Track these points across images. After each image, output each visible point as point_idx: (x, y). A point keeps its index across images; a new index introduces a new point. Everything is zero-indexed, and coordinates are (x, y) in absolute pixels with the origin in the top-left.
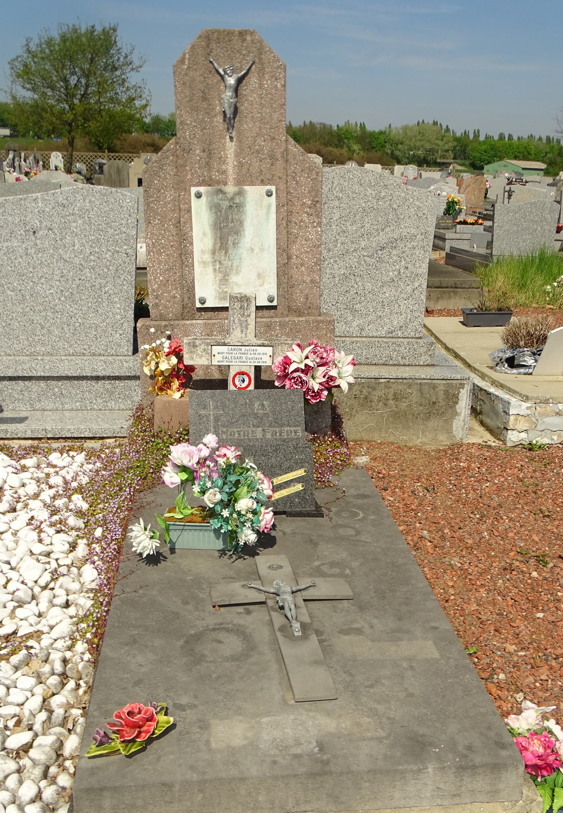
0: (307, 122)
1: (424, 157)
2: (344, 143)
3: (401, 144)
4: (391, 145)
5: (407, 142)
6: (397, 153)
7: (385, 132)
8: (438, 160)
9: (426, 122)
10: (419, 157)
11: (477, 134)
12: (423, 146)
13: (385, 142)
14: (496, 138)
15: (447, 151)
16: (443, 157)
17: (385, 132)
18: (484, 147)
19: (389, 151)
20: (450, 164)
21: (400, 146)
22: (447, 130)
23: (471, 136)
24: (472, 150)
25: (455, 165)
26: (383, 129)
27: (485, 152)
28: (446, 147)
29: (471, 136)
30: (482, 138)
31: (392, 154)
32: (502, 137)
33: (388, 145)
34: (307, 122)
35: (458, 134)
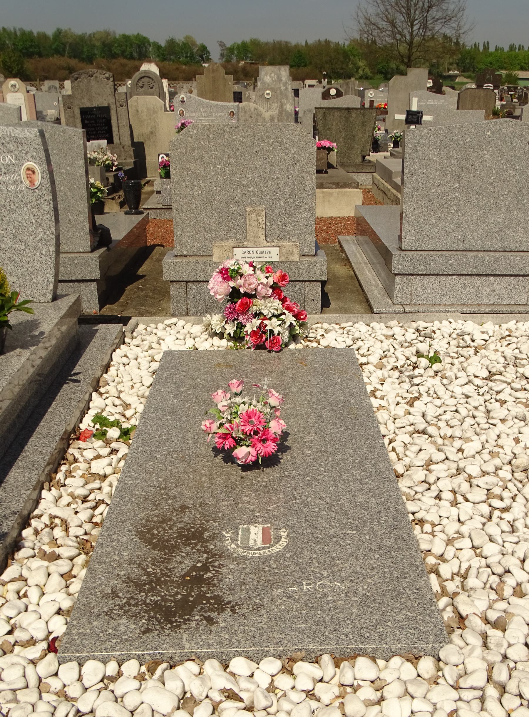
2: (350, 60)
8: (444, 74)
18: (490, 59)
20: (456, 76)
24: (478, 62)
25: (461, 78)
27: (491, 63)
31: (397, 69)
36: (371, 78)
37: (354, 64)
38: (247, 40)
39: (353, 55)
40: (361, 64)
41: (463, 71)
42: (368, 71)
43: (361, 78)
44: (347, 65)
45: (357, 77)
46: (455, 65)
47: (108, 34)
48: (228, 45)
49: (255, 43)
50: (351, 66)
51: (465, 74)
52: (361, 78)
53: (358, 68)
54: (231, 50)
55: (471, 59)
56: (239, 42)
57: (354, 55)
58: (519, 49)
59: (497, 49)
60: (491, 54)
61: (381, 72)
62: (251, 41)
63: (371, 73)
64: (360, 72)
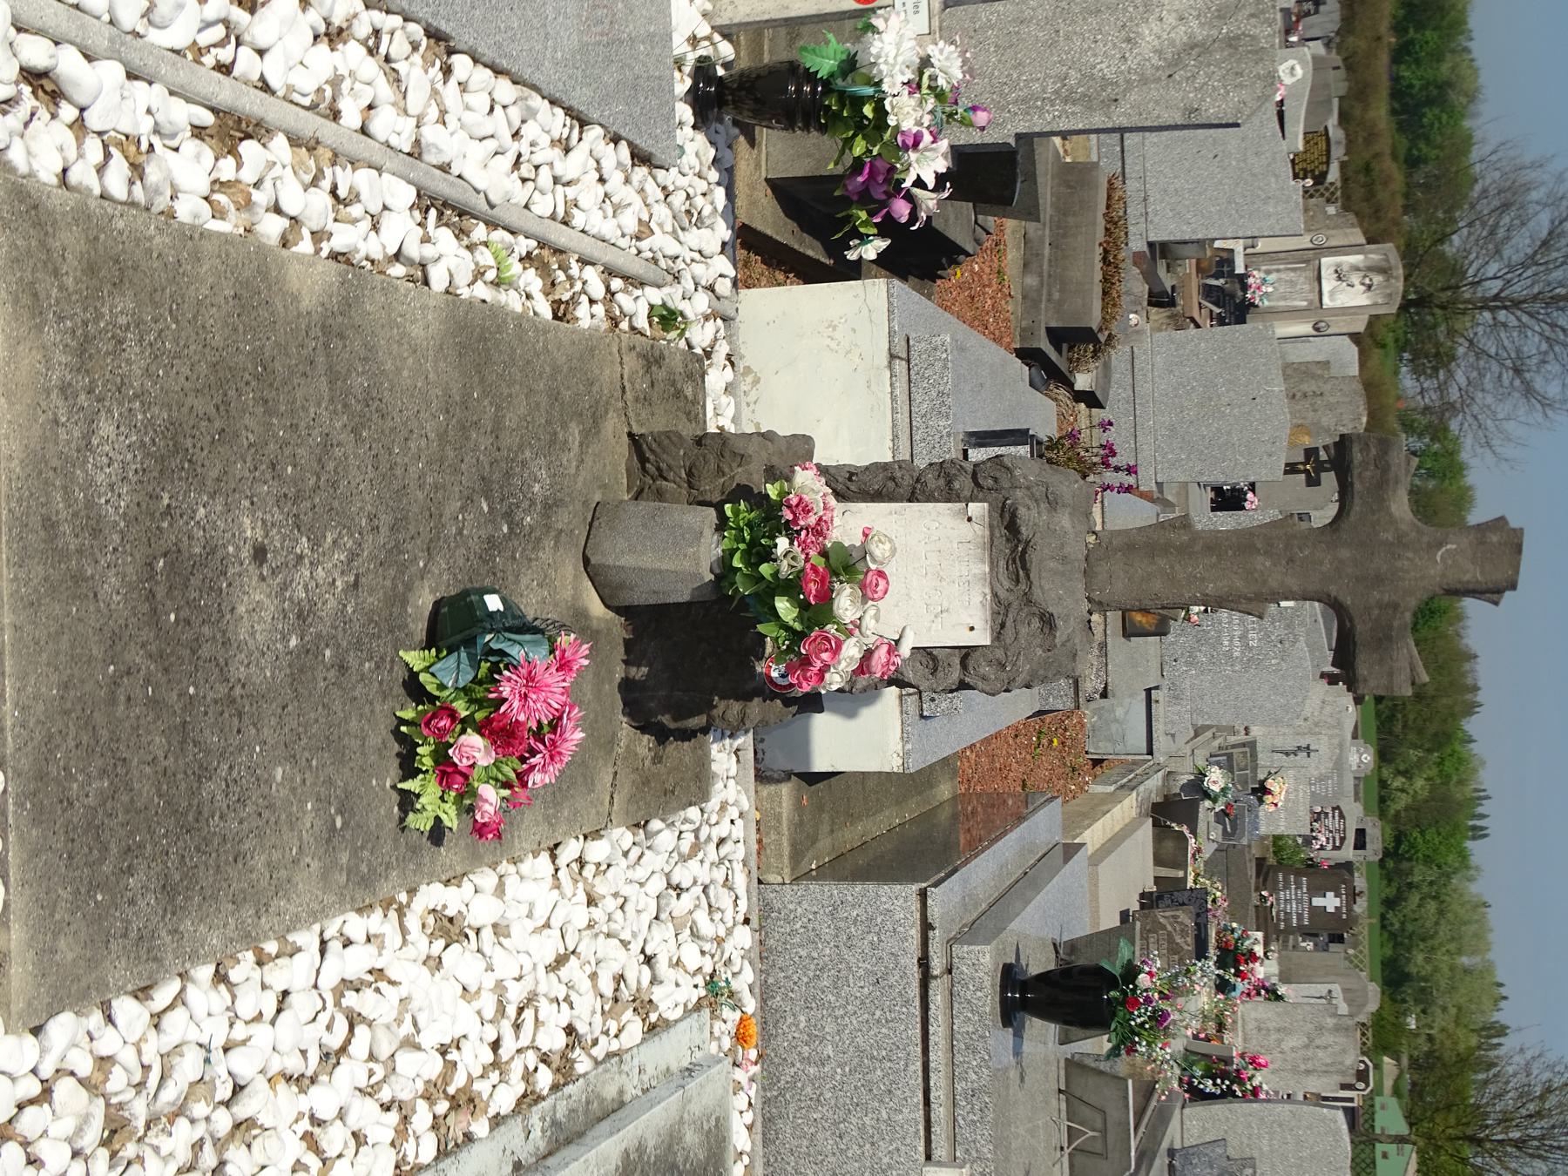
1: (1406, 977)
2: (1429, 751)
3: (1441, 913)
4: (1431, 883)
5: (1444, 930)
6: (1415, 898)
7: (1468, 867)
9: (1503, 1004)
10: (1408, 960)
12: (1436, 970)
13: (1439, 867)
17: (1468, 867)
19: (1417, 878)
21: (1432, 906)
25: (1395, 1071)
26: (1474, 860)
31: (1410, 885)
33: (1432, 874)
37: (1420, 764)
39: (1440, 763)
40: (1419, 783)
42: (1401, 802)
43: (1383, 784)
44: (1416, 747)
45: (1385, 773)
50: (1414, 754)
52: (1383, 784)
53: (1407, 774)
57: (1440, 763)
61: (1398, 840)
62: (1470, 488)
63: (1398, 813)
64: (1398, 782)
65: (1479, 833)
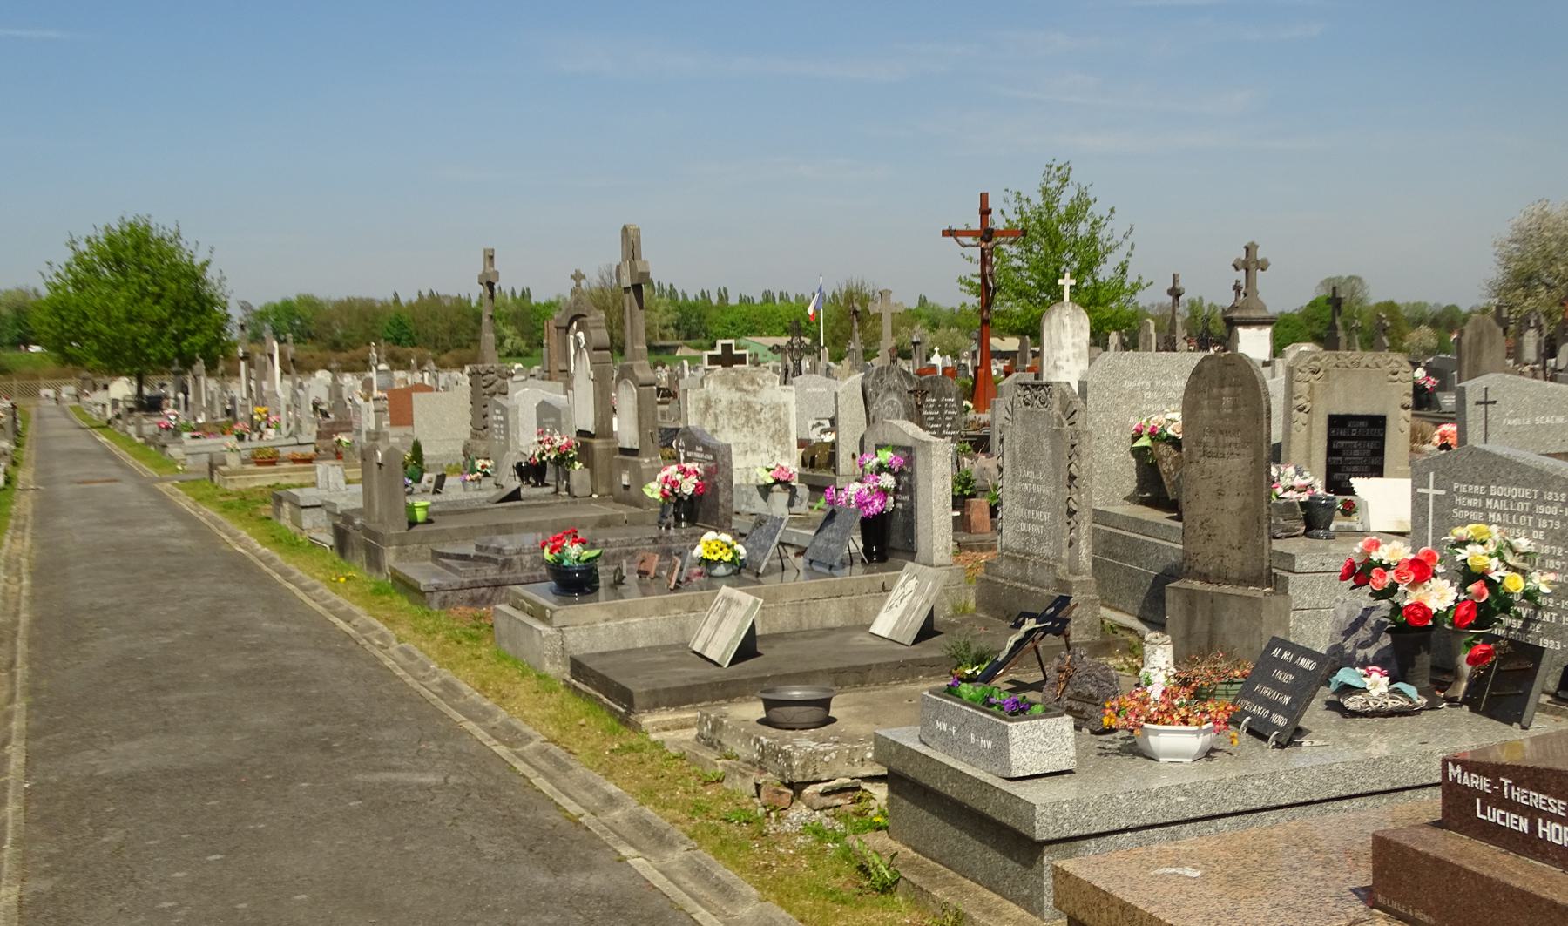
0: (426, 293)
11: (723, 296)
14: (758, 299)
15: (666, 327)
16: (663, 337)
18: (731, 317)
20: (676, 347)
22: (673, 291)
23: (715, 299)
26: (553, 299)
28: (664, 322)
29: (715, 299)
30: (733, 301)
32: (768, 297)
34: (426, 293)
35: (691, 298)
36: (527, 355)
38: (293, 297)
40: (507, 331)
41: (688, 337)
46: (672, 330)
47: (25, 294)
48: (257, 307)
49: (310, 302)
51: (692, 342)
54: (262, 316)
55: (699, 316)
56: (278, 300)
58: (781, 298)
59: (741, 300)
60: (733, 308)
65: (526, 294)
